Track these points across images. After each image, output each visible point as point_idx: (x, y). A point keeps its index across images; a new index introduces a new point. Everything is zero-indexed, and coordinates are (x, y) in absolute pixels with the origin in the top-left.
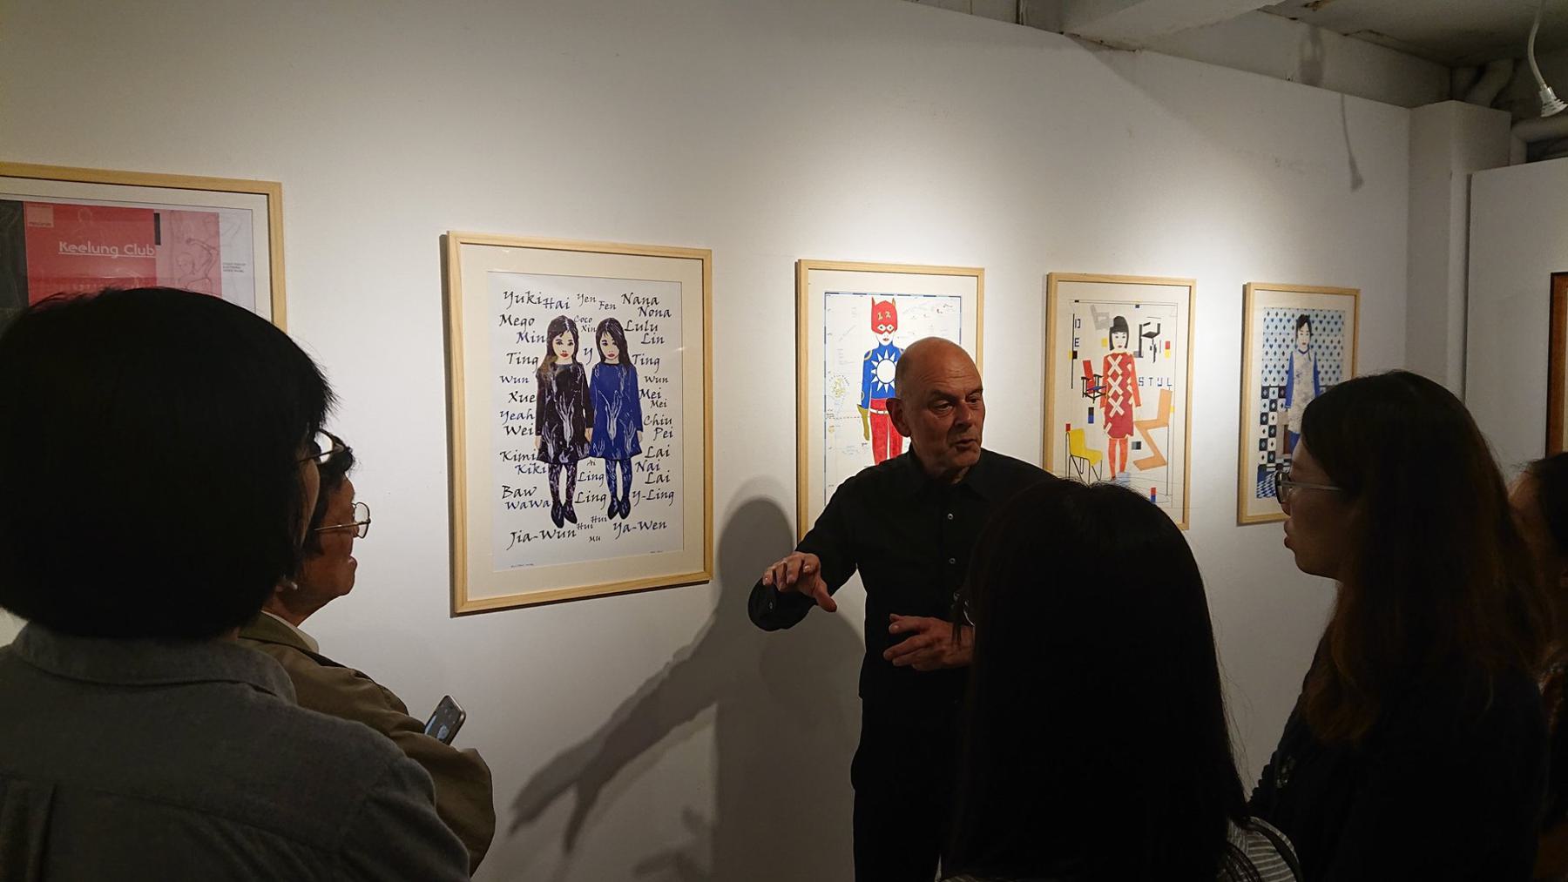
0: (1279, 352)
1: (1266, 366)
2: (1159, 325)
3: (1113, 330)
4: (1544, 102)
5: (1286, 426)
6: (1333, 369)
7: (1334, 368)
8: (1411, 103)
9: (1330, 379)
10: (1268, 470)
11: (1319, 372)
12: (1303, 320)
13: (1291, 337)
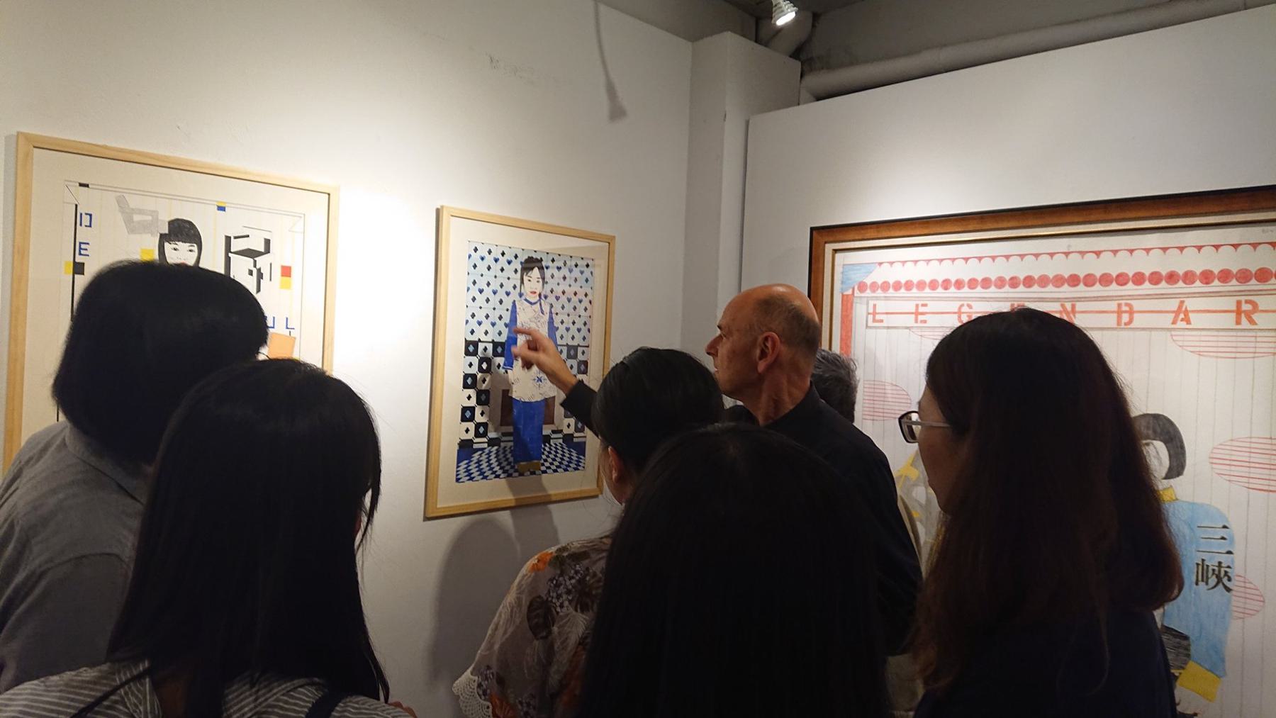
0: (494, 300)
1: (473, 316)
2: (267, 242)
3: (164, 238)
4: (774, 4)
5: (506, 394)
6: (577, 326)
7: (579, 324)
8: (693, 41)
9: (573, 338)
10: (475, 446)
11: (557, 328)
12: (531, 264)
13: (511, 283)
